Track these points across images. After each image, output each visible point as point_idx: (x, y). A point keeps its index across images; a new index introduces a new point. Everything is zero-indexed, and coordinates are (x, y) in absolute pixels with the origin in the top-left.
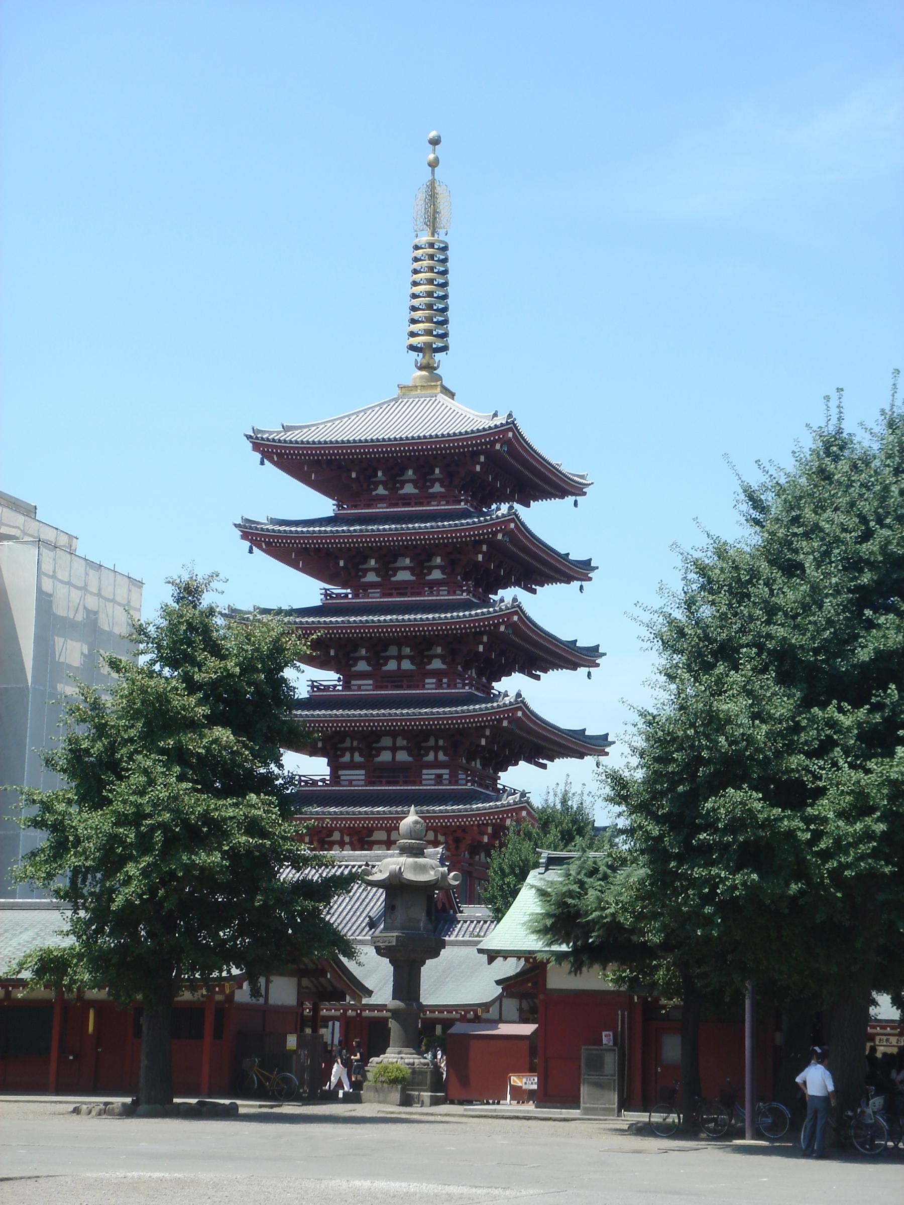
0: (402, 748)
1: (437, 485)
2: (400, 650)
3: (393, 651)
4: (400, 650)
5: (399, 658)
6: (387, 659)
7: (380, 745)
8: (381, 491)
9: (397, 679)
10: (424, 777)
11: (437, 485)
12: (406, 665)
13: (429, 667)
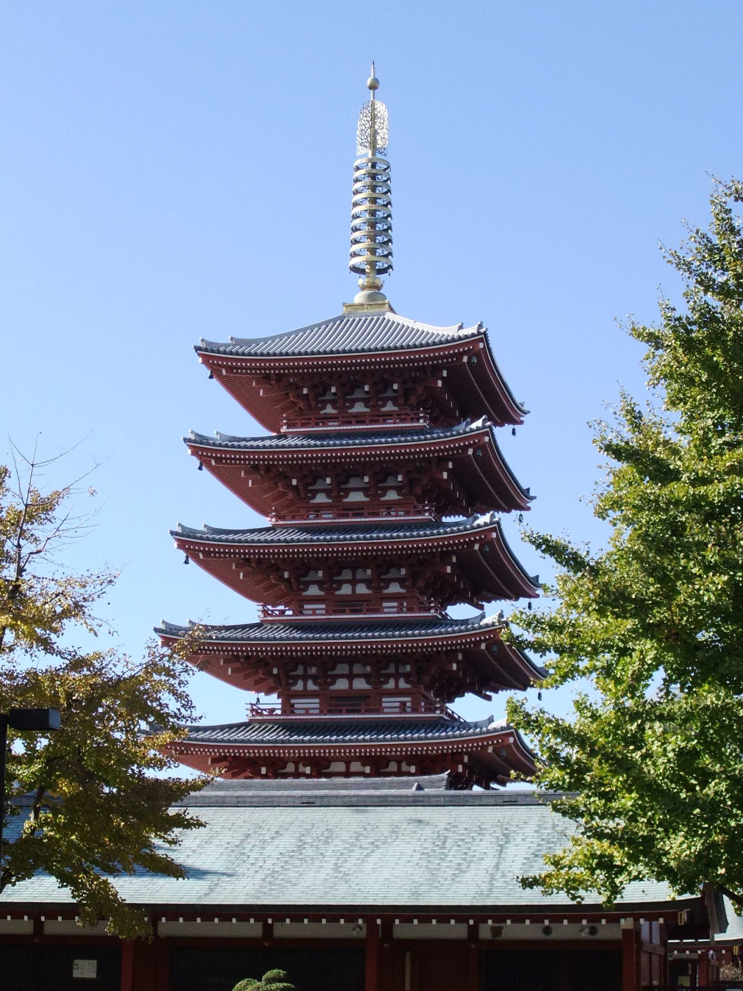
0: (359, 676)
1: (390, 403)
2: (354, 575)
3: (347, 574)
4: (354, 575)
5: (354, 582)
6: (340, 584)
7: (335, 672)
8: (329, 410)
9: (354, 603)
10: (384, 705)
11: (390, 403)
12: (362, 589)
13: (385, 591)
